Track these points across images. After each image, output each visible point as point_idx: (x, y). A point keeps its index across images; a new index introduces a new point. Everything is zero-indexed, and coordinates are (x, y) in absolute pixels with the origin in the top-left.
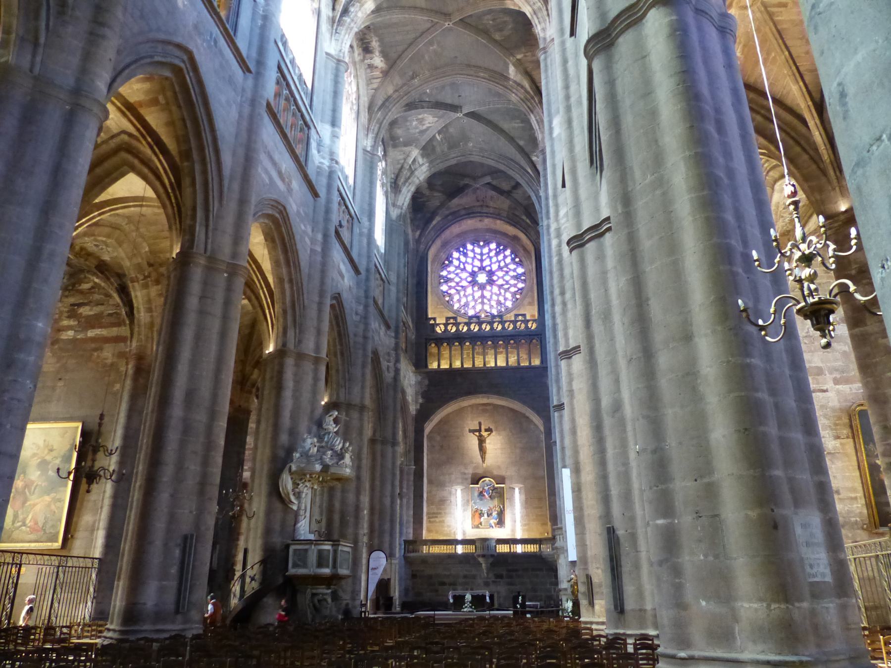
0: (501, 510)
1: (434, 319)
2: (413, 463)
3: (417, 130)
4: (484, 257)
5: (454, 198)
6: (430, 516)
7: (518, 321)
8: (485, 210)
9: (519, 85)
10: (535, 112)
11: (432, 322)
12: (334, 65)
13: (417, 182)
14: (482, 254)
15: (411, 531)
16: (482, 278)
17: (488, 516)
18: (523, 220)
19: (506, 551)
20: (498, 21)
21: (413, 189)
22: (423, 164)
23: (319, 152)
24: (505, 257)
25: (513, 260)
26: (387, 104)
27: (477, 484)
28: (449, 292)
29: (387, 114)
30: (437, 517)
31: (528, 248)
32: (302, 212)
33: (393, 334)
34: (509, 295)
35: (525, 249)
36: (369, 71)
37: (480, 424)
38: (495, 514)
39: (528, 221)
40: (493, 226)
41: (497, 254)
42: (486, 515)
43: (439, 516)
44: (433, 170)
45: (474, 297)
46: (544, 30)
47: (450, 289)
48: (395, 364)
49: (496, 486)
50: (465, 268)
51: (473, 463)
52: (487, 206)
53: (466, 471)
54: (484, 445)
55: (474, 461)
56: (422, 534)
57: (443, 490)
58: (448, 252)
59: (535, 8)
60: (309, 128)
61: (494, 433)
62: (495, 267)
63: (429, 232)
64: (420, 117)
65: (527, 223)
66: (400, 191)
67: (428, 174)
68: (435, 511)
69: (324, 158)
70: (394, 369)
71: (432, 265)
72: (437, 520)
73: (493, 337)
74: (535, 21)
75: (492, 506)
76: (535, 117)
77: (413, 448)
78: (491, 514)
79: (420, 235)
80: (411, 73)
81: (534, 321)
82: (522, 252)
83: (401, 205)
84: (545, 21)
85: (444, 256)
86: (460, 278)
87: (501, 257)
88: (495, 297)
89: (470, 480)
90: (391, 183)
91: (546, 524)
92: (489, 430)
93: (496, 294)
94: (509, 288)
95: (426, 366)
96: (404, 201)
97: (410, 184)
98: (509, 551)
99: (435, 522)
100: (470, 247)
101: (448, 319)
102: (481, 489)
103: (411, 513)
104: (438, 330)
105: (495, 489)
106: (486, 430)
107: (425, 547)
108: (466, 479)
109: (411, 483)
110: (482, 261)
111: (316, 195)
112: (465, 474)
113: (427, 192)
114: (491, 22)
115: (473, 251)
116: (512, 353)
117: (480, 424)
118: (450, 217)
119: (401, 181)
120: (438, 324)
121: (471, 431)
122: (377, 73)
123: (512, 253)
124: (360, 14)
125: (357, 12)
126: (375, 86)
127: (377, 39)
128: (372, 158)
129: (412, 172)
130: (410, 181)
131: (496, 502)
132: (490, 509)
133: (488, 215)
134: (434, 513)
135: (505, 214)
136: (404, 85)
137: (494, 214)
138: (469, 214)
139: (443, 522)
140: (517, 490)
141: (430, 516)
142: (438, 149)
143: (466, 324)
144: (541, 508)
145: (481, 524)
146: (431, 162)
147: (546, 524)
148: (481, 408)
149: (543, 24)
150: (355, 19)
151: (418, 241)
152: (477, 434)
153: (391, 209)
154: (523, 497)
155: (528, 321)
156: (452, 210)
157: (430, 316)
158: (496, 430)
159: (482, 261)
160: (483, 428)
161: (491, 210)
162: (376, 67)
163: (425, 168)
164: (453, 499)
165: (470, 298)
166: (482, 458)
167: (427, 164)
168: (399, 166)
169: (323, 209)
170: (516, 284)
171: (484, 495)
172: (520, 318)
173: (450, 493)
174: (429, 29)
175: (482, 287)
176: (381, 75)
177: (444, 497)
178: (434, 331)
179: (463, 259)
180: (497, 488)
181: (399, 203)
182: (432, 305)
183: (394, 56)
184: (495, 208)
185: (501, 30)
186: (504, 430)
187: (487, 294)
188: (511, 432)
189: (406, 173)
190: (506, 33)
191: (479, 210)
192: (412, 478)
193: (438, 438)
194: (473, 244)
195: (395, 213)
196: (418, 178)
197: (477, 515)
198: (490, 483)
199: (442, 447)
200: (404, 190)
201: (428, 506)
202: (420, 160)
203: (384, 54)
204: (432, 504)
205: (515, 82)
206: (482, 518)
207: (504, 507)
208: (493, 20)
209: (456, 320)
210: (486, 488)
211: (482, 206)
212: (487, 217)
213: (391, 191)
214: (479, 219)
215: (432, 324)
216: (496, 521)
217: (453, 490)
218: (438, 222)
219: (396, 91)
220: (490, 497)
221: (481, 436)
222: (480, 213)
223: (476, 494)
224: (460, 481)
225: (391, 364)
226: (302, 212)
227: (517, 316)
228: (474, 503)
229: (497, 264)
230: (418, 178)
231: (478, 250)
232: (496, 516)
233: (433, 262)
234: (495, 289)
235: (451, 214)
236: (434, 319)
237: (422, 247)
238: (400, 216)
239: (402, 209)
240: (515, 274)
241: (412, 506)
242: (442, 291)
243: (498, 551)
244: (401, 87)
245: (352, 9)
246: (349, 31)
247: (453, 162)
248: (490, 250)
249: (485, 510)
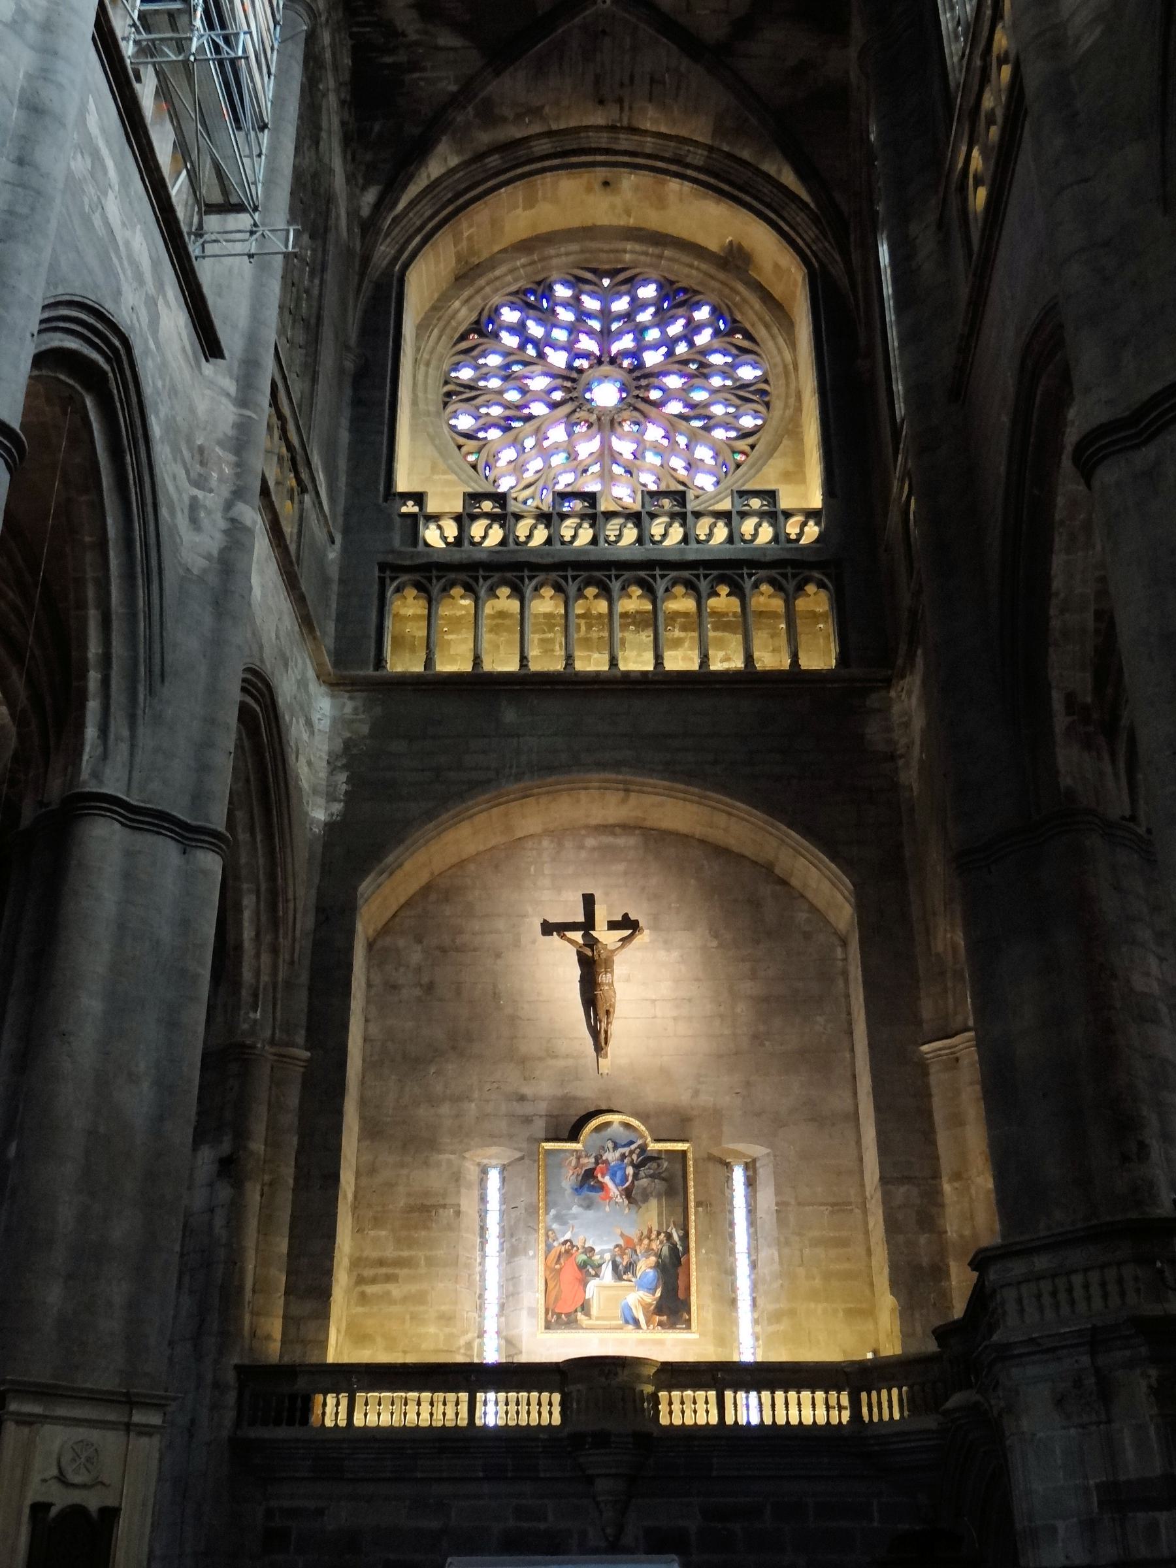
0: (673, 1248)
1: (419, 498)
2: (300, 1037)
4: (615, 326)
6: (368, 1273)
7: (743, 515)
8: (625, 142)
11: (410, 508)
14: (606, 315)
15: (275, 1327)
16: (606, 395)
17: (618, 1273)
18: (767, 177)
19: (701, 1421)
24: (693, 328)
25: (717, 333)
27: (573, 1136)
28: (481, 435)
30: (389, 1278)
31: (777, 291)
33: (231, 387)
34: (703, 453)
35: (767, 297)
37: (589, 902)
38: (646, 1266)
39: (789, 178)
40: (654, 220)
41: (662, 320)
42: (607, 1271)
43: (403, 1272)
45: (572, 456)
47: (485, 428)
48: (228, 506)
49: (654, 1146)
50: (541, 355)
51: (556, 1057)
52: (633, 130)
53: (527, 1090)
54: (603, 978)
55: (562, 1046)
56: (323, 1344)
57: (426, 1163)
58: (478, 300)
61: (644, 938)
62: (652, 358)
63: (412, 204)
68: (390, 1253)
70: (222, 524)
71: (418, 337)
72: (395, 1290)
73: (649, 565)
75: (633, 1233)
77: (304, 978)
78: (631, 1267)
79: (380, 206)
81: (811, 514)
82: (758, 305)
85: (465, 316)
86: (524, 391)
87: (675, 329)
88: (652, 459)
89: (539, 1127)
91: (868, 1312)
92: (627, 924)
93: (657, 449)
94: (707, 429)
95: (379, 662)
98: (714, 1419)
99: (386, 1297)
100: (562, 292)
101: (474, 498)
102: (589, 1162)
103: (284, 1247)
104: (431, 535)
105: (646, 1159)
106: (613, 925)
107: (331, 1399)
108: (528, 1120)
109: (289, 1119)
110: (606, 336)
112: (522, 1098)
115: (574, 304)
116: (721, 644)
117: (589, 902)
118: (494, 161)
120: (435, 518)
121: (548, 928)
123: (716, 312)
131: (652, 1214)
132: (628, 1245)
134: (381, 1263)
137: (662, 159)
139: (420, 1298)
140: (738, 1175)
141: (368, 1273)
143: (545, 518)
144: (843, 1243)
145: (585, 1307)
147: (868, 1312)
148: (590, 842)
151: (369, 228)
152: (577, 936)
154: (767, 1197)
155: (788, 515)
157: (403, 484)
158: (655, 928)
159: (606, 336)
160: (602, 915)
161: (649, 145)
164: (468, 1204)
165: (558, 459)
166: (595, 1033)
170: (737, 417)
171: (601, 1187)
172: (756, 503)
173: (457, 1177)
175: (606, 423)
177: (426, 1194)
178: (414, 536)
179: (535, 330)
180: (655, 1158)
182: (413, 456)
186: (689, 927)
187: (624, 447)
188: (716, 936)
191: (603, 140)
192: (293, 1099)
193: (416, 956)
194: (576, 282)
197: (570, 1272)
198: (626, 1135)
199: (430, 988)
201: (359, 1230)
204: (377, 1222)
206: (593, 1284)
207: (685, 1238)
209: (503, 506)
210: (611, 1156)
214: (602, 173)
215: (413, 517)
216: (650, 1299)
217: (471, 1170)
218: (452, 171)
220: (628, 1193)
221: (591, 942)
222: (607, 151)
223: (568, 1179)
224: (502, 1125)
225: (212, 500)
227: (743, 494)
228: (560, 1219)
229: (664, 350)
231: (591, 304)
232: (651, 1273)
233: (423, 327)
234: (654, 433)
236: (419, 498)
237: (384, 250)
240: (729, 383)
241: (284, 1217)
242: (453, 428)
243: (664, 1420)
248: (638, 305)
249: (604, 1247)
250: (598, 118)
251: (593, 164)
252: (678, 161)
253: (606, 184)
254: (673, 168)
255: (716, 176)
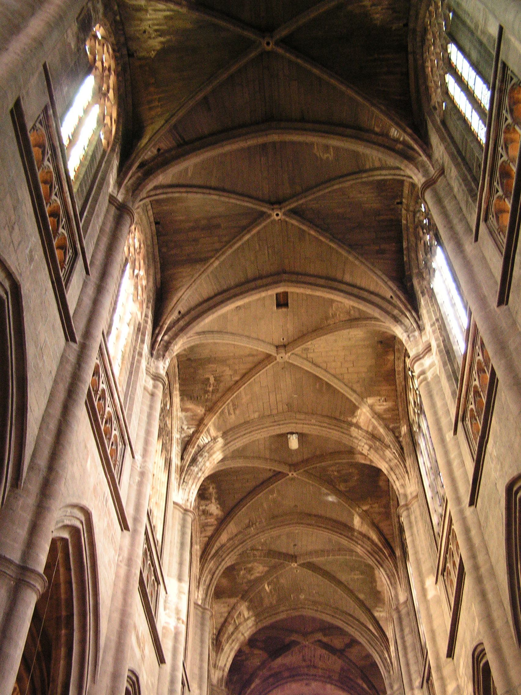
3: (245, 580)
5: (277, 657)
8: (313, 671)
9: (364, 536)
10: (384, 566)
12: (181, 515)
13: (242, 638)
18: (358, 685)
20: (344, 472)
21: (236, 647)
22: (248, 618)
23: (165, 608)
26: (220, 553)
29: (220, 564)
32: (149, 682)
36: (203, 517)
39: (365, 686)
44: (260, 626)
46: (403, 486)
52: (315, 667)
59: (392, 464)
60: (158, 583)
64: (250, 566)
65: (362, 688)
66: (223, 649)
67: (254, 630)
69: (170, 617)
74: (392, 477)
76: (385, 571)
80: (247, 521)
83: (223, 665)
84: (403, 477)
90: (213, 639)
96: (227, 661)
97: (233, 641)
111: (161, 660)
113: (247, 650)
114: (336, 473)
118: (271, 680)
119: (223, 639)
122: (212, 520)
124: (208, 464)
125: (205, 462)
126: (209, 533)
127: (214, 485)
128: (203, 613)
129: (236, 628)
130: (233, 637)
133: (315, 677)
135: (336, 677)
136: (240, 532)
138: (293, 676)
142: (266, 602)
146: (257, 615)
149: (402, 481)
150: (203, 469)
153: (212, 671)
156: (273, 672)
161: (320, 672)
162: (211, 514)
163: (250, 623)
167: (253, 618)
168: (223, 620)
169: (168, 678)
174: (270, 478)
176: (216, 523)
181: (221, 664)
183: (230, 503)
184: (323, 669)
185: (346, 481)
189: (231, 628)
190: (351, 484)
195: (216, 676)
196: (243, 634)
200: (227, 648)
202: (246, 614)
203: (221, 501)
205: (360, 533)
208: (338, 471)
211: (308, 667)
212: (316, 680)
213: (213, 649)
214: (305, 682)
219: (230, 539)
226: (149, 682)
230: (243, 634)
235: (271, 676)
238: (220, 680)
239: (223, 671)
244: (236, 535)
245: (200, 459)
246: (196, 480)
247: (282, 616)
250: (304, 664)
251: (303, 679)
252: (329, 677)
253: (307, 684)
254: (328, 680)
255: (342, 684)
